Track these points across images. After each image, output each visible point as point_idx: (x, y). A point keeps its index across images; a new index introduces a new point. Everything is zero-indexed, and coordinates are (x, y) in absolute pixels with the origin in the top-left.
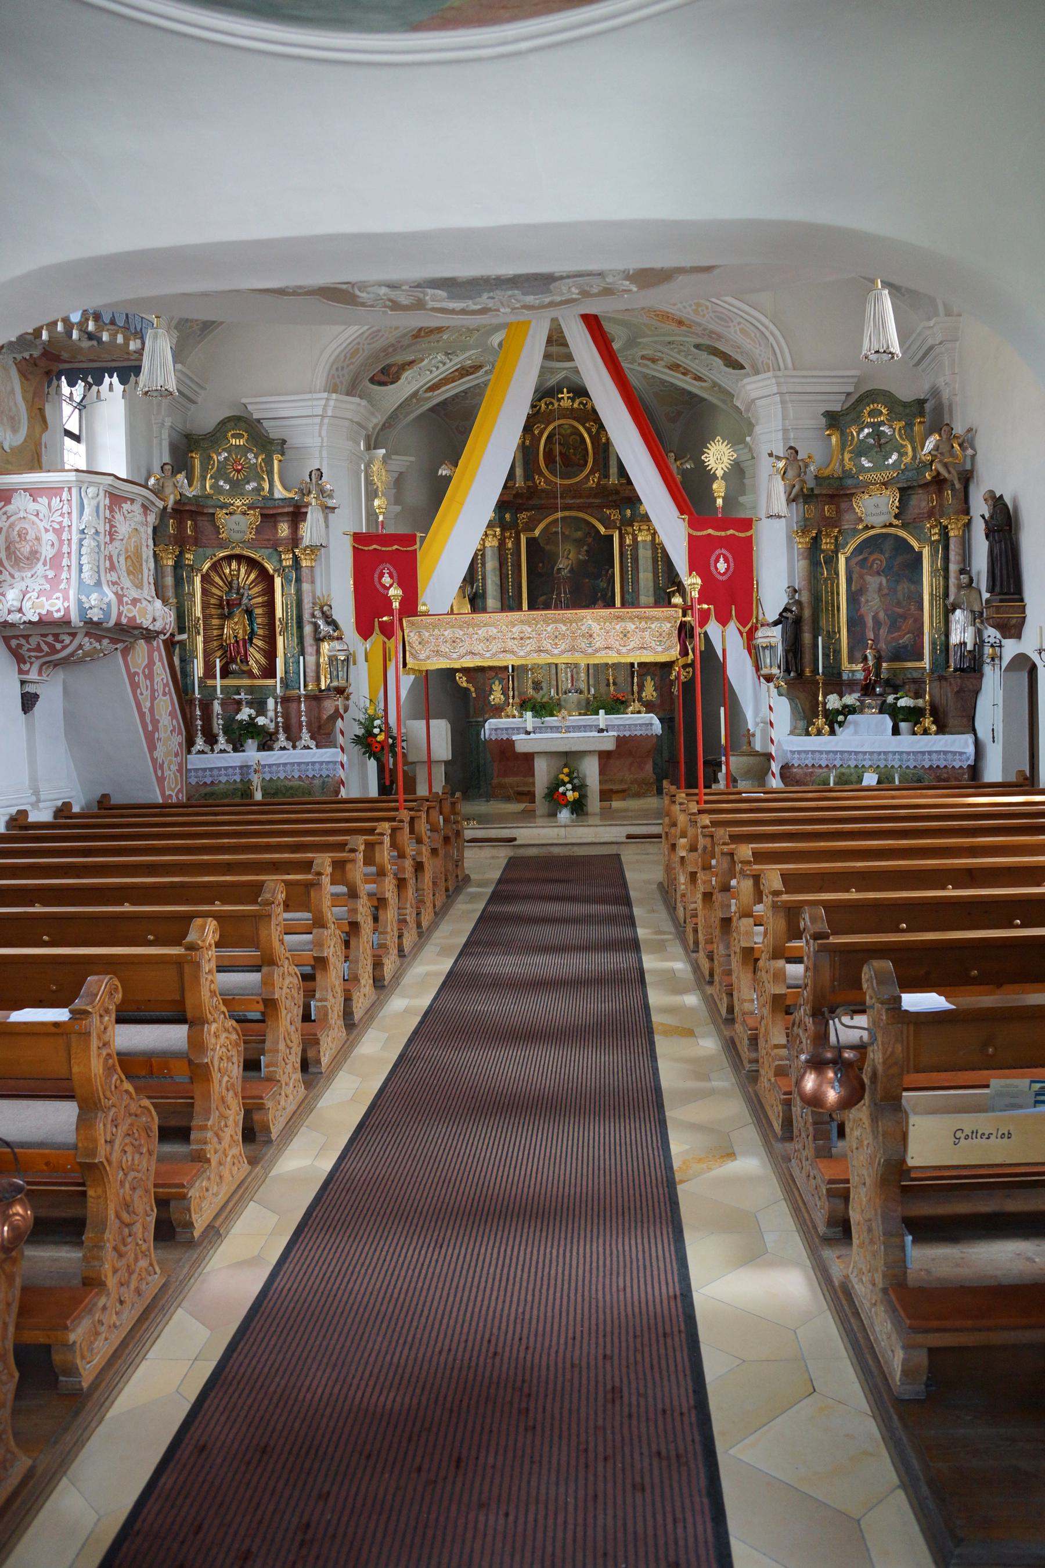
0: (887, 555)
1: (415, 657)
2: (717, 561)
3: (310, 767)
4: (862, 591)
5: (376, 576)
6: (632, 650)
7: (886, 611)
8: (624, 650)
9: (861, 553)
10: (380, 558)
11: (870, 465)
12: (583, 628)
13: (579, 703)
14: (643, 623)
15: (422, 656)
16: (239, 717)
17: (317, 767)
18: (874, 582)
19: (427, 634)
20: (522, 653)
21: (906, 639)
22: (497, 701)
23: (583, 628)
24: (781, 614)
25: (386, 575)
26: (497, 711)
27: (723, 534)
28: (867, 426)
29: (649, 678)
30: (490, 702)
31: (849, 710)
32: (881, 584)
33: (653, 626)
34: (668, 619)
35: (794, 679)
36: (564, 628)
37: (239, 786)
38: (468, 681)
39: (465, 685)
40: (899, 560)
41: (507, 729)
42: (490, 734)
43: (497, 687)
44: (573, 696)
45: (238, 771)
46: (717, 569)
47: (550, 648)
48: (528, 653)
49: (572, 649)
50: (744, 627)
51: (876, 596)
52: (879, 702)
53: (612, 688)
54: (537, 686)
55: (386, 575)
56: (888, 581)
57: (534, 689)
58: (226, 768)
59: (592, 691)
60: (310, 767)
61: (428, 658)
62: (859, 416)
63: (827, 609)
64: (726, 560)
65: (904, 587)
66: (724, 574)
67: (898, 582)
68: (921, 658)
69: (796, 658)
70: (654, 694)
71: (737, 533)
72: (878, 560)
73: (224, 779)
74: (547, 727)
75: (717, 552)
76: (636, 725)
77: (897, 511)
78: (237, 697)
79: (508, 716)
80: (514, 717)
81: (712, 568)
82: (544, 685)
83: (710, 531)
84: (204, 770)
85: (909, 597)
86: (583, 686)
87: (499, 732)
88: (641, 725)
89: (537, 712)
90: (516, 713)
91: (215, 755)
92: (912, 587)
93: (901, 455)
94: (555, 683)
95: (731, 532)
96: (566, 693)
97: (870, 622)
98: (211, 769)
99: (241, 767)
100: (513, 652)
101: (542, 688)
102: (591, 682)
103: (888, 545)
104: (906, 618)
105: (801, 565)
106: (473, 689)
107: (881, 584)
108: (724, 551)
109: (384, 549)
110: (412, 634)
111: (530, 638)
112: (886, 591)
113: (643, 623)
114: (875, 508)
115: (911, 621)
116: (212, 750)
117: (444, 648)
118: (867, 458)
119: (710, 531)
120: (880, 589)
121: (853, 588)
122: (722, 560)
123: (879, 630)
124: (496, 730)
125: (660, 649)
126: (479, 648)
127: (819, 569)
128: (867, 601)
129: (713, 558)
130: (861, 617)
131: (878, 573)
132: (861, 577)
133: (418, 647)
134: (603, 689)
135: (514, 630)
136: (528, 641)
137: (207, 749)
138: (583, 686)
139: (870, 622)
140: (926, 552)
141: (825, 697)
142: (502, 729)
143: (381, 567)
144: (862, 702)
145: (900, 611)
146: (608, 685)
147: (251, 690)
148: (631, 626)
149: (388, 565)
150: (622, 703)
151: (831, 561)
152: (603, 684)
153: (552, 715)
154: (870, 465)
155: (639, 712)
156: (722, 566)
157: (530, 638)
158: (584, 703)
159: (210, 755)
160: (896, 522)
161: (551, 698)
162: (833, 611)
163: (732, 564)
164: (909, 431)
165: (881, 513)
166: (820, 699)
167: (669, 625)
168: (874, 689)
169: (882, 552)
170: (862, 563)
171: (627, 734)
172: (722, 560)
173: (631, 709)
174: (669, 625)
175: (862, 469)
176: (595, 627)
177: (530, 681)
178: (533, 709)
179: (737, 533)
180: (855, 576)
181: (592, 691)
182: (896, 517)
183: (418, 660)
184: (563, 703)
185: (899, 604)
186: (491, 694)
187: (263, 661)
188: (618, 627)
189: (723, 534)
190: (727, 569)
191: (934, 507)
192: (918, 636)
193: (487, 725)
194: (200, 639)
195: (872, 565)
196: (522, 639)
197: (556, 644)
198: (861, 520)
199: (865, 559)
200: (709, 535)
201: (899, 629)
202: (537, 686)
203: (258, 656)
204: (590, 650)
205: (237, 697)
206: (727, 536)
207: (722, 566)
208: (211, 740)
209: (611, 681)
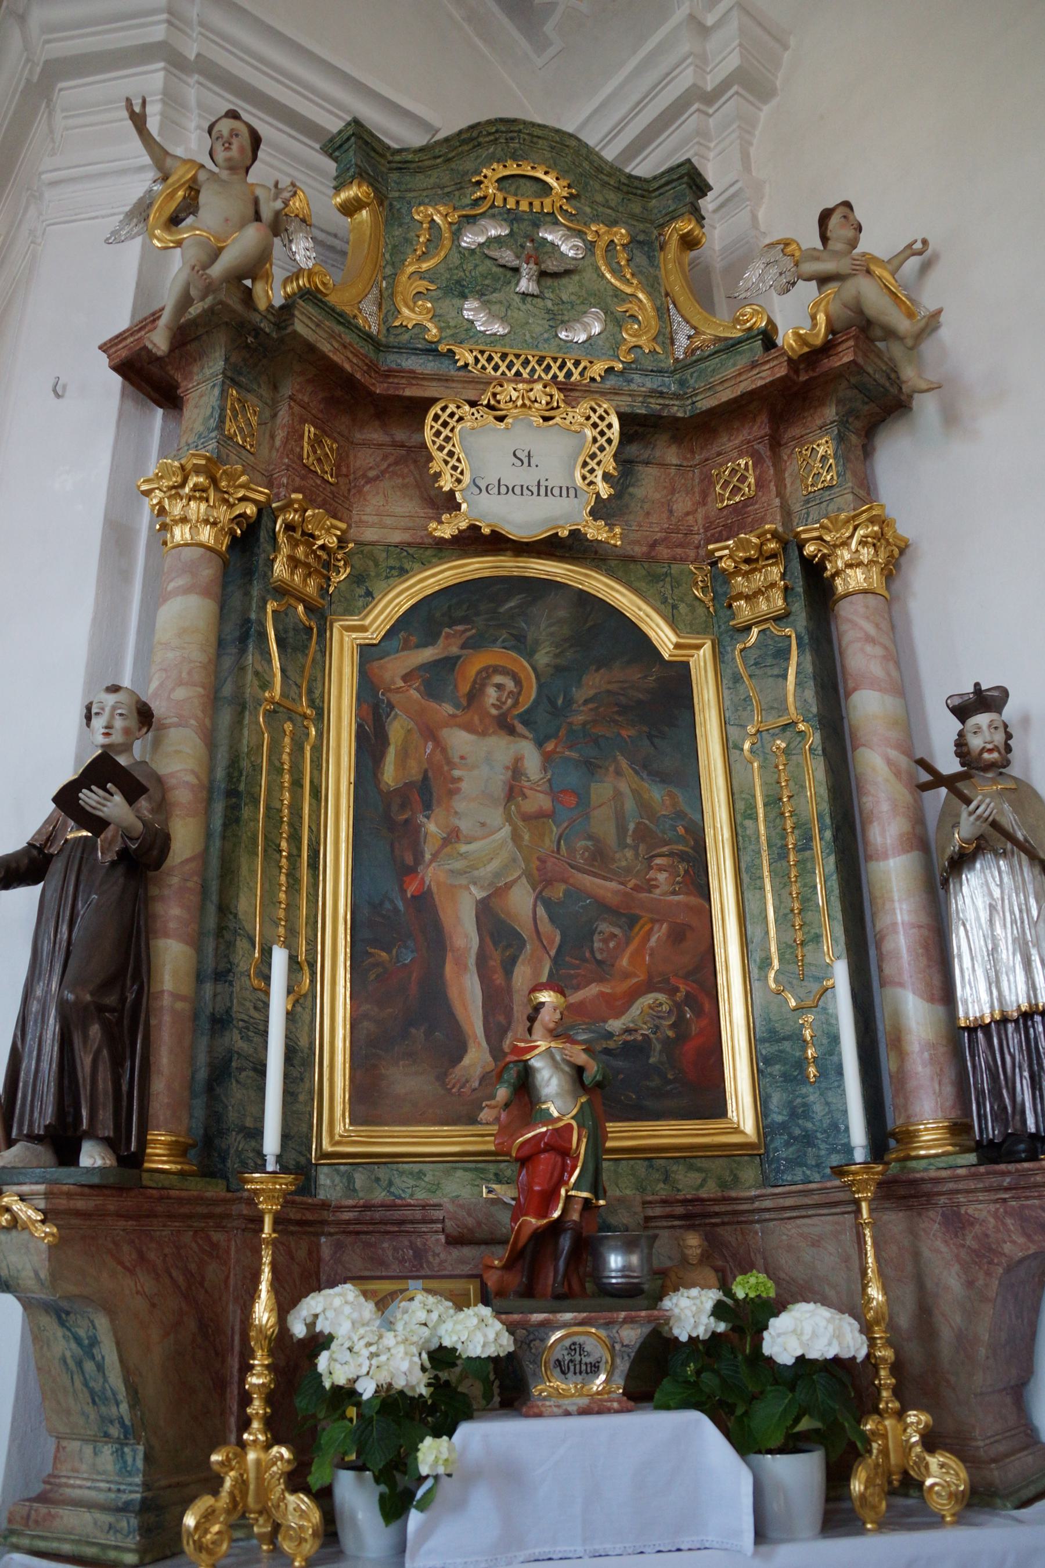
0: (543, 657)
4: (428, 790)
7: (542, 881)
9: (430, 638)
11: (498, 328)
18: (484, 762)
21: (640, 1015)
24: (67, 799)
28: (496, 213)
31: (457, 1391)
32: (516, 770)
35: (99, 1186)
40: (594, 683)
51: (495, 816)
52: (631, 1335)
56: (548, 759)
62: (464, 182)
63: (272, 847)
65: (619, 791)
67: (591, 768)
68: (710, 1101)
69: (117, 1063)
72: (509, 674)
77: (604, 490)
85: (643, 834)
92: (656, 794)
93: (616, 321)
97: (464, 932)
103: (546, 628)
104: (632, 921)
105: (186, 615)
107: (516, 770)
112: (539, 801)
114: (522, 467)
115: (660, 933)
118: (486, 304)
120: (513, 792)
121: (390, 774)
123: (509, 966)
127: (251, 658)
128: (453, 837)
130: (424, 903)
131: (505, 725)
132: (430, 733)
139: (464, 932)
140: (702, 662)
141: (284, 1306)
144: (527, 1338)
145: (608, 888)
151: (304, 642)
154: (498, 328)
160: (595, 531)
162: (294, 858)
164: (640, 259)
165: (542, 489)
166: (263, 1313)
168: (587, 1250)
169: (521, 644)
170: (436, 678)
175: (467, 332)
180: (397, 729)
182: (600, 510)
185: (599, 859)
191: (749, 501)
192: (690, 1000)
195: (475, 695)
198: (449, 503)
199: (448, 664)
201: (603, 970)
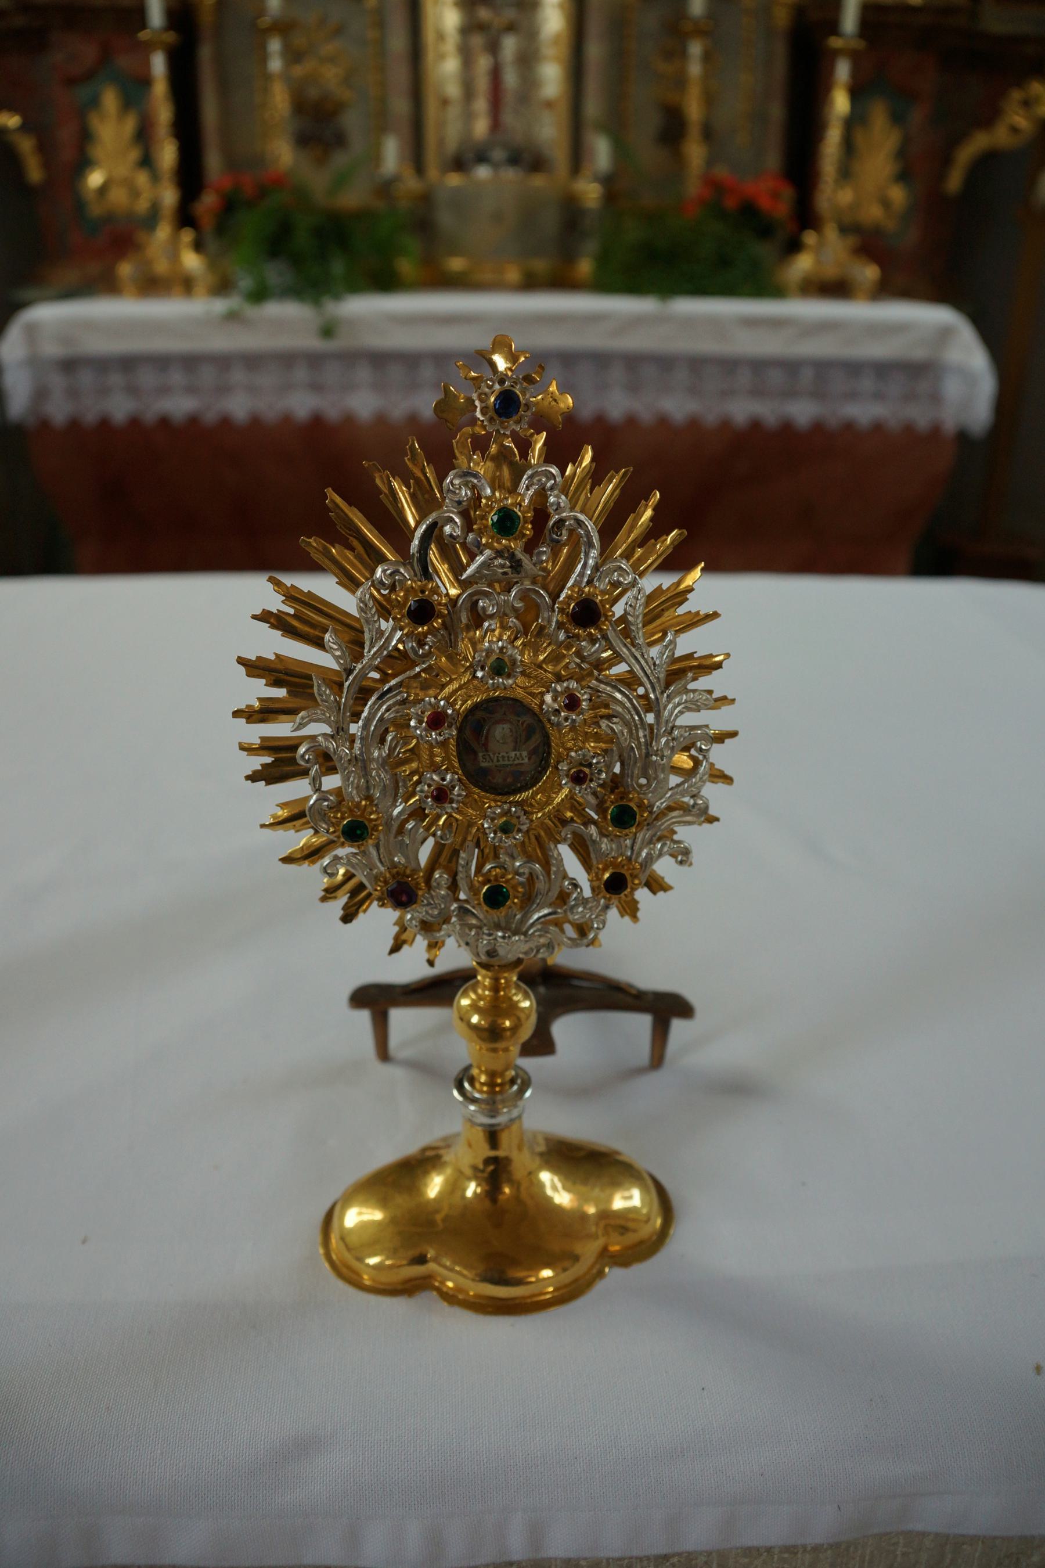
22: (118, 197)
29: (879, 115)
30: (79, 205)
41: (128, 363)
42: (40, 394)
43: (111, 129)
53: (695, 152)
54: (319, 125)
57: (303, 140)
59: (601, 152)
70: (898, 194)
74: (351, 358)
76: (854, 368)
79: (151, 285)
80: (187, 285)
82: (352, 121)
86: (549, 132)
87: (86, 378)
88: (883, 369)
89: (297, 261)
90: (191, 261)
94: (400, 106)
96: (459, 164)
101: (340, 140)
102: (593, 107)
106: (26, 145)
124: (69, 365)
134: (648, 154)
138: (549, 132)
142: (102, 364)
150: (764, 229)
152: (646, 125)
153: (386, 282)
155: (836, 288)
158: (550, 221)
161: (385, 189)
171: (803, 412)
173: (803, 264)
177: (280, 100)
178: (278, 243)
181: (601, 152)
184: (445, 219)
186: (83, 163)
202: (319, 125)
209: (694, 110)
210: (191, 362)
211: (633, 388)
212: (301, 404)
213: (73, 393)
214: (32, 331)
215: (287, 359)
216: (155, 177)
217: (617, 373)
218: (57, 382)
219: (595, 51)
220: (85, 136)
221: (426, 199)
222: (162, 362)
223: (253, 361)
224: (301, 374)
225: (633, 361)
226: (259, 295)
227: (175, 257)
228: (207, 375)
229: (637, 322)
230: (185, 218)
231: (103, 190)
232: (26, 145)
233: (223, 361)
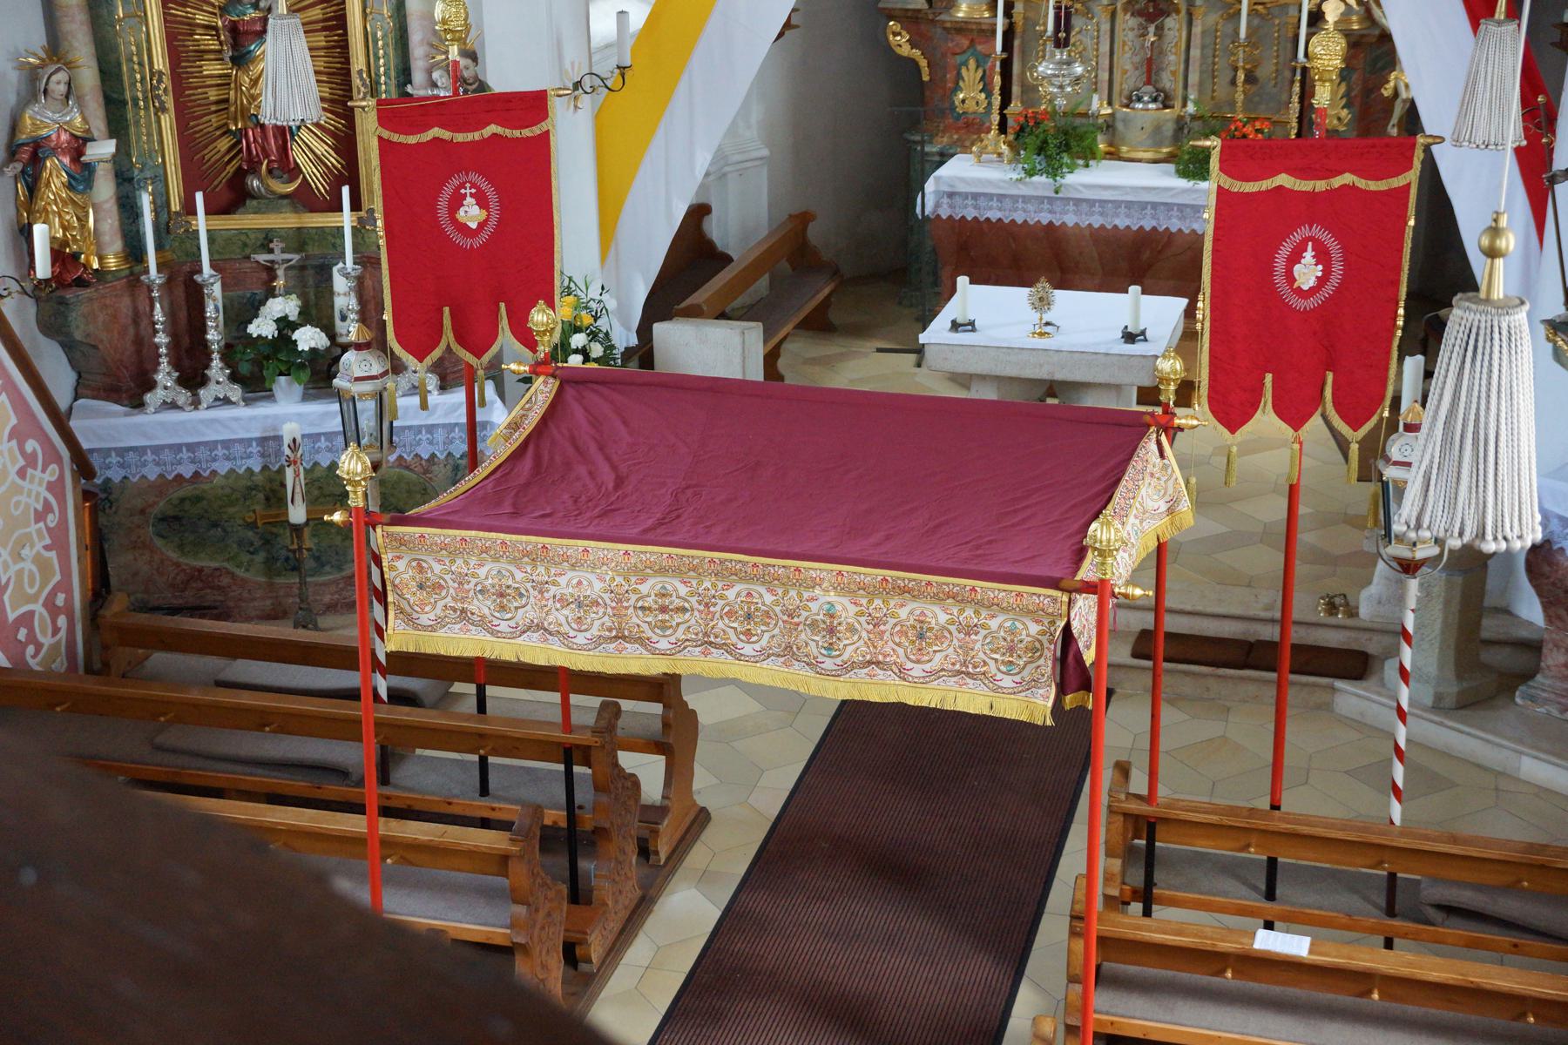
1: (410, 620)
2: (1296, 257)
3: (424, 436)
5: (443, 203)
6: (935, 674)
8: (917, 671)
10: (448, 159)
12: (814, 606)
13: (1157, 129)
14: (969, 612)
15: (424, 620)
16: (254, 329)
17: (440, 436)
19: (437, 568)
20: (663, 644)
22: (970, 106)
23: (814, 606)
25: (469, 200)
26: (969, 131)
27: (1320, 185)
30: (953, 108)
33: (994, 624)
34: (1034, 613)
36: (769, 598)
37: (259, 479)
38: (913, 44)
39: (905, 50)
41: (975, 196)
42: (937, 205)
43: (971, 74)
44: (1147, 112)
45: (255, 449)
46: (1291, 278)
47: (734, 639)
48: (680, 646)
49: (789, 652)
50: (1355, 427)
55: (469, 200)
58: (227, 444)
60: (424, 436)
61: (440, 623)
64: (1322, 256)
66: (1313, 291)
70: (1344, 113)
71: (1361, 183)
73: (223, 468)
75: (1297, 237)
78: (262, 258)
81: (1279, 279)
83: (1284, 180)
84: (177, 448)
87: (958, 200)
91: (203, 414)
95: (1347, 178)
98: (191, 447)
99: (263, 441)
100: (641, 641)
106: (923, 63)
108: (1317, 231)
109: (460, 137)
110: (401, 565)
111: (684, 610)
113: (969, 612)
116: (196, 403)
117: (482, 606)
119: (1284, 180)
122: (1309, 256)
124: (951, 195)
125: (1007, 682)
126: (561, 617)
129: (1285, 250)
133: (413, 596)
135: (644, 589)
136: (678, 618)
137: (183, 396)
142: (965, 196)
143: (455, 182)
146: (1233, 82)
147: (299, 240)
148: (939, 616)
149: (474, 177)
156: (1307, 272)
157: (684, 610)
158: (1169, 129)
159: (189, 416)
163: (1337, 268)
167: (1034, 628)
172: (1309, 256)
174: (1034, 628)
176: (846, 609)
179: (1361, 183)
183: (417, 627)
184: (1120, 126)
186: (957, 88)
187: (332, 159)
188: (903, 613)
189: (1320, 185)
190: (1322, 281)
193: (930, 186)
194: (167, 121)
196: (664, 609)
197: (748, 633)
200: (1280, 188)
203: (320, 148)
204: (829, 664)
205: (262, 258)
206: (1330, 193)
207: (1307, 272)
208: (193, 379)
210: (1001, 197)
211: (1182, 218)
212: (1045, 218)
213: (951, 206)
214: (938, 179)
215: (1041, 199)
216: (989, 95)
217: (1175, 213)
218: (945, 200)
219: (1195, 53)
220: (959, 77)
221: (1112, 115)
222: (990, 196)
223: (1026, 199)
224: (1046, 206)
225: (1181, 207)
226: (1030, 173)
227: (996, 144)
228: (1008, 203)
229: (1185, 191)
230: (1003, 128)
231: (963, 101)
232: (923, 63)
233: (1014, 198)
